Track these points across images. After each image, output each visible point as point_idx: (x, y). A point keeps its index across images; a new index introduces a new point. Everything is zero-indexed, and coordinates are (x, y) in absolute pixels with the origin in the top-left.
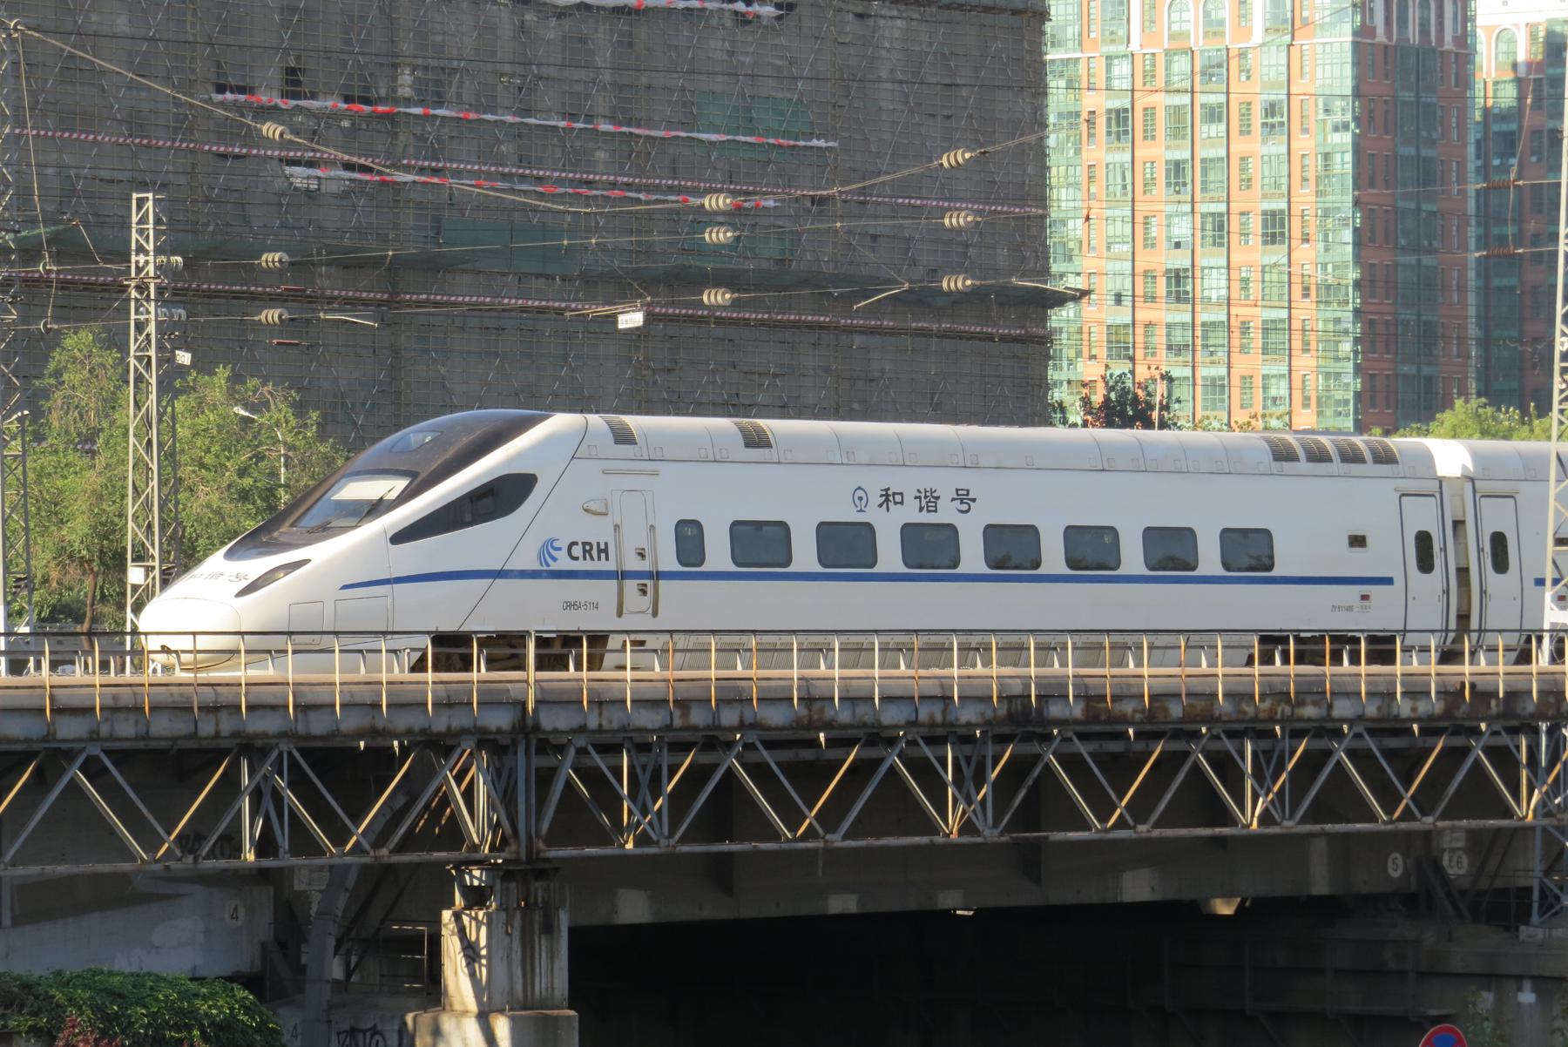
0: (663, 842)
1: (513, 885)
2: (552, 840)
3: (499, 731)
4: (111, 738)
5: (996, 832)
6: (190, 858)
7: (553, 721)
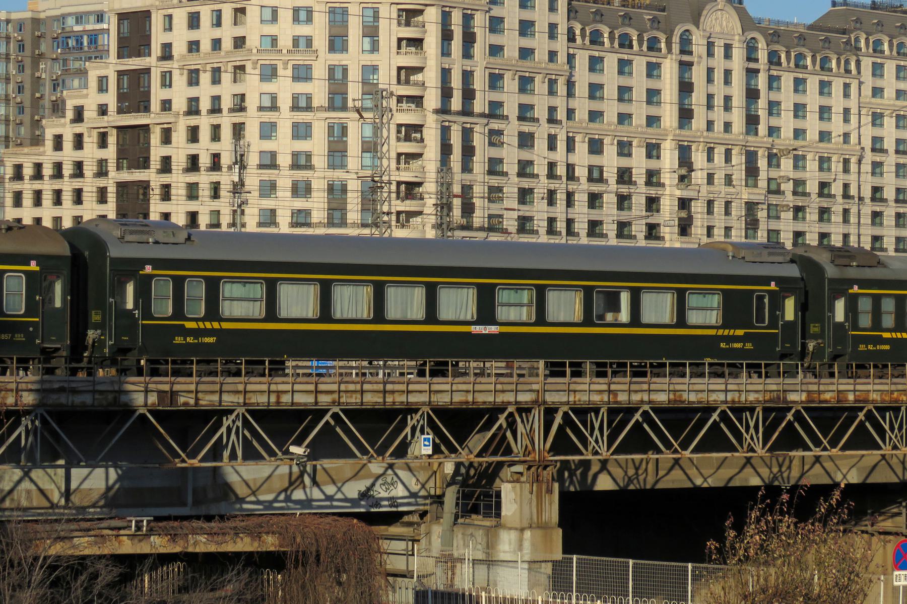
0: (604, 454)
7: (550, 398)
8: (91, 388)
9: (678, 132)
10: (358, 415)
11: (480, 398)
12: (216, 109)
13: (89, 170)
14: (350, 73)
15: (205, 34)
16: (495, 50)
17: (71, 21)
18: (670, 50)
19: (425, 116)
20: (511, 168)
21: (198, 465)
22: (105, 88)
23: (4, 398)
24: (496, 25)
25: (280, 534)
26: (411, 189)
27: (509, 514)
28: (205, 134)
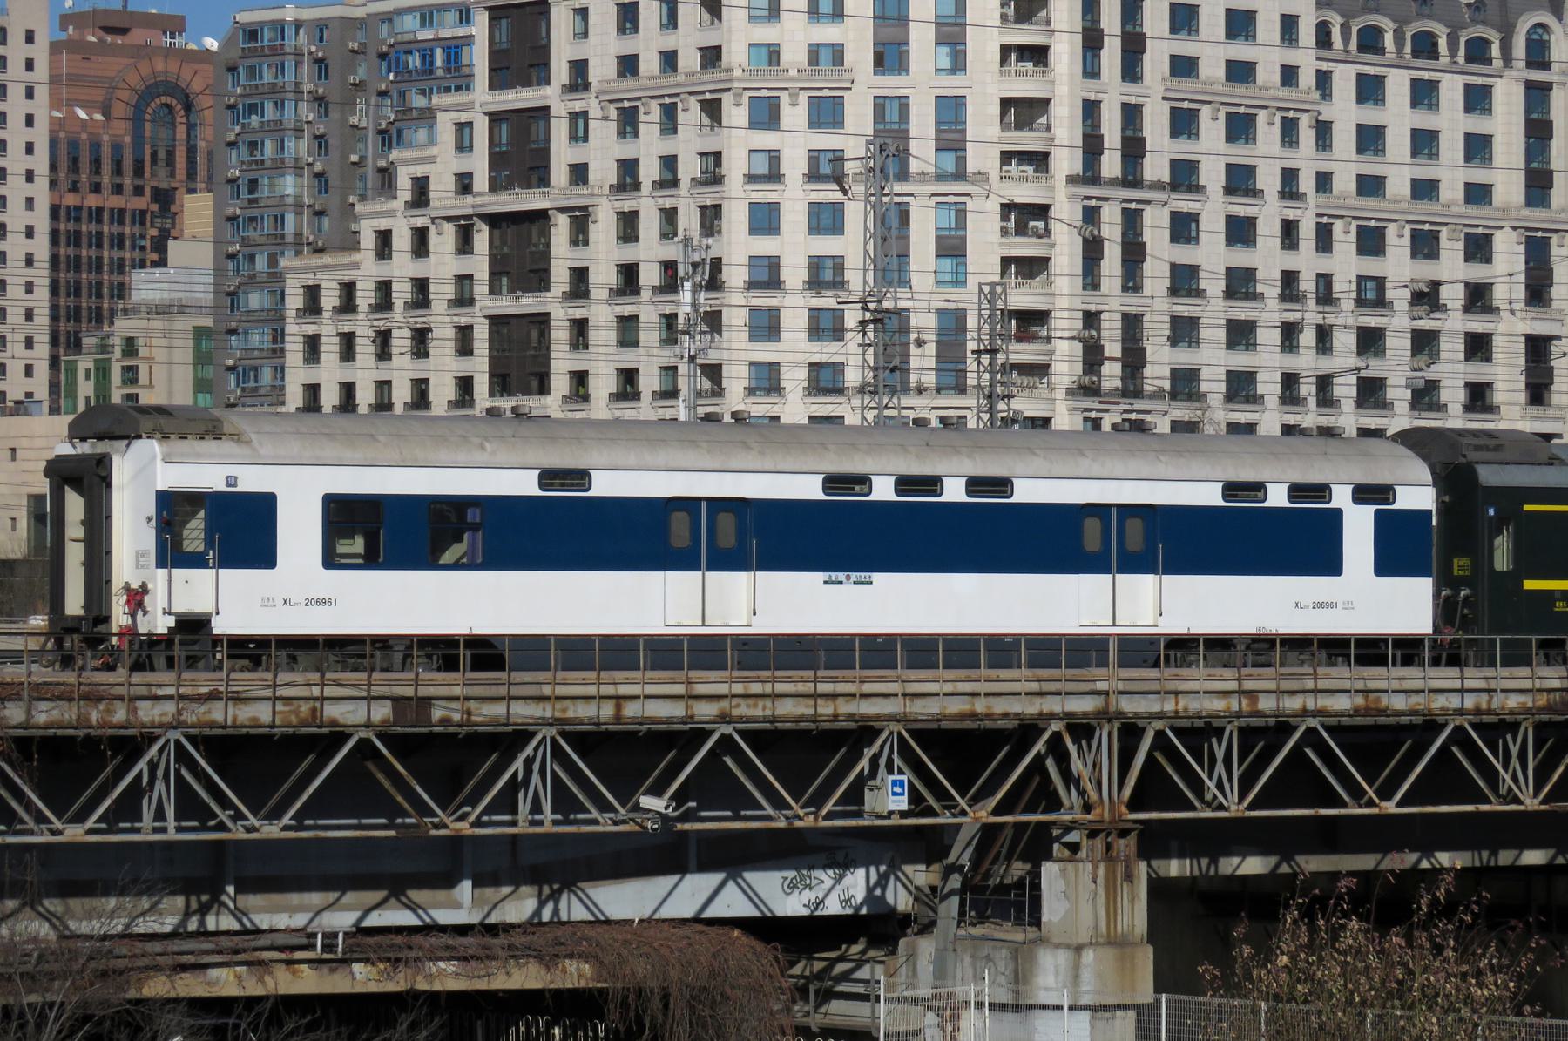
0: (1234, 807)
1: (1099, 842)
2: (1134, 805)
3: (1085, 715)
4: (741, 719)
5: (1536, 801)
6: (811, 817)
7: (1129, 706)
8: (268, 693)
9: (1526, 212)
10: (769, 740)
11: (1000, 706)
12: (669, 181)
13: (442, 292)
14: (913, 110)
15: (649, 43)
16: (1183, 66)
17: (410, 23)
18: (1507, 59)
19: (1052, 189)
20: (1213, 285)
21: (470, 832)
22: (466, 144)
23: (108, 711)
24: (1184, 19)
25: (596, 957)
26: (1031, 322)
27: (1056, 919)
28: (649, 225)
